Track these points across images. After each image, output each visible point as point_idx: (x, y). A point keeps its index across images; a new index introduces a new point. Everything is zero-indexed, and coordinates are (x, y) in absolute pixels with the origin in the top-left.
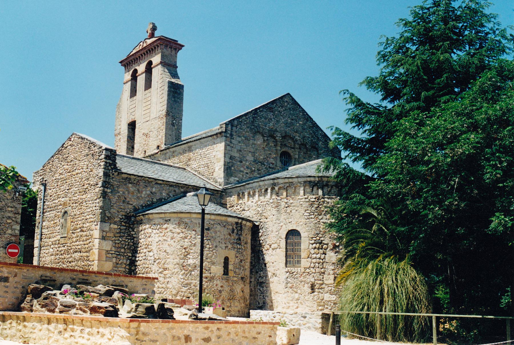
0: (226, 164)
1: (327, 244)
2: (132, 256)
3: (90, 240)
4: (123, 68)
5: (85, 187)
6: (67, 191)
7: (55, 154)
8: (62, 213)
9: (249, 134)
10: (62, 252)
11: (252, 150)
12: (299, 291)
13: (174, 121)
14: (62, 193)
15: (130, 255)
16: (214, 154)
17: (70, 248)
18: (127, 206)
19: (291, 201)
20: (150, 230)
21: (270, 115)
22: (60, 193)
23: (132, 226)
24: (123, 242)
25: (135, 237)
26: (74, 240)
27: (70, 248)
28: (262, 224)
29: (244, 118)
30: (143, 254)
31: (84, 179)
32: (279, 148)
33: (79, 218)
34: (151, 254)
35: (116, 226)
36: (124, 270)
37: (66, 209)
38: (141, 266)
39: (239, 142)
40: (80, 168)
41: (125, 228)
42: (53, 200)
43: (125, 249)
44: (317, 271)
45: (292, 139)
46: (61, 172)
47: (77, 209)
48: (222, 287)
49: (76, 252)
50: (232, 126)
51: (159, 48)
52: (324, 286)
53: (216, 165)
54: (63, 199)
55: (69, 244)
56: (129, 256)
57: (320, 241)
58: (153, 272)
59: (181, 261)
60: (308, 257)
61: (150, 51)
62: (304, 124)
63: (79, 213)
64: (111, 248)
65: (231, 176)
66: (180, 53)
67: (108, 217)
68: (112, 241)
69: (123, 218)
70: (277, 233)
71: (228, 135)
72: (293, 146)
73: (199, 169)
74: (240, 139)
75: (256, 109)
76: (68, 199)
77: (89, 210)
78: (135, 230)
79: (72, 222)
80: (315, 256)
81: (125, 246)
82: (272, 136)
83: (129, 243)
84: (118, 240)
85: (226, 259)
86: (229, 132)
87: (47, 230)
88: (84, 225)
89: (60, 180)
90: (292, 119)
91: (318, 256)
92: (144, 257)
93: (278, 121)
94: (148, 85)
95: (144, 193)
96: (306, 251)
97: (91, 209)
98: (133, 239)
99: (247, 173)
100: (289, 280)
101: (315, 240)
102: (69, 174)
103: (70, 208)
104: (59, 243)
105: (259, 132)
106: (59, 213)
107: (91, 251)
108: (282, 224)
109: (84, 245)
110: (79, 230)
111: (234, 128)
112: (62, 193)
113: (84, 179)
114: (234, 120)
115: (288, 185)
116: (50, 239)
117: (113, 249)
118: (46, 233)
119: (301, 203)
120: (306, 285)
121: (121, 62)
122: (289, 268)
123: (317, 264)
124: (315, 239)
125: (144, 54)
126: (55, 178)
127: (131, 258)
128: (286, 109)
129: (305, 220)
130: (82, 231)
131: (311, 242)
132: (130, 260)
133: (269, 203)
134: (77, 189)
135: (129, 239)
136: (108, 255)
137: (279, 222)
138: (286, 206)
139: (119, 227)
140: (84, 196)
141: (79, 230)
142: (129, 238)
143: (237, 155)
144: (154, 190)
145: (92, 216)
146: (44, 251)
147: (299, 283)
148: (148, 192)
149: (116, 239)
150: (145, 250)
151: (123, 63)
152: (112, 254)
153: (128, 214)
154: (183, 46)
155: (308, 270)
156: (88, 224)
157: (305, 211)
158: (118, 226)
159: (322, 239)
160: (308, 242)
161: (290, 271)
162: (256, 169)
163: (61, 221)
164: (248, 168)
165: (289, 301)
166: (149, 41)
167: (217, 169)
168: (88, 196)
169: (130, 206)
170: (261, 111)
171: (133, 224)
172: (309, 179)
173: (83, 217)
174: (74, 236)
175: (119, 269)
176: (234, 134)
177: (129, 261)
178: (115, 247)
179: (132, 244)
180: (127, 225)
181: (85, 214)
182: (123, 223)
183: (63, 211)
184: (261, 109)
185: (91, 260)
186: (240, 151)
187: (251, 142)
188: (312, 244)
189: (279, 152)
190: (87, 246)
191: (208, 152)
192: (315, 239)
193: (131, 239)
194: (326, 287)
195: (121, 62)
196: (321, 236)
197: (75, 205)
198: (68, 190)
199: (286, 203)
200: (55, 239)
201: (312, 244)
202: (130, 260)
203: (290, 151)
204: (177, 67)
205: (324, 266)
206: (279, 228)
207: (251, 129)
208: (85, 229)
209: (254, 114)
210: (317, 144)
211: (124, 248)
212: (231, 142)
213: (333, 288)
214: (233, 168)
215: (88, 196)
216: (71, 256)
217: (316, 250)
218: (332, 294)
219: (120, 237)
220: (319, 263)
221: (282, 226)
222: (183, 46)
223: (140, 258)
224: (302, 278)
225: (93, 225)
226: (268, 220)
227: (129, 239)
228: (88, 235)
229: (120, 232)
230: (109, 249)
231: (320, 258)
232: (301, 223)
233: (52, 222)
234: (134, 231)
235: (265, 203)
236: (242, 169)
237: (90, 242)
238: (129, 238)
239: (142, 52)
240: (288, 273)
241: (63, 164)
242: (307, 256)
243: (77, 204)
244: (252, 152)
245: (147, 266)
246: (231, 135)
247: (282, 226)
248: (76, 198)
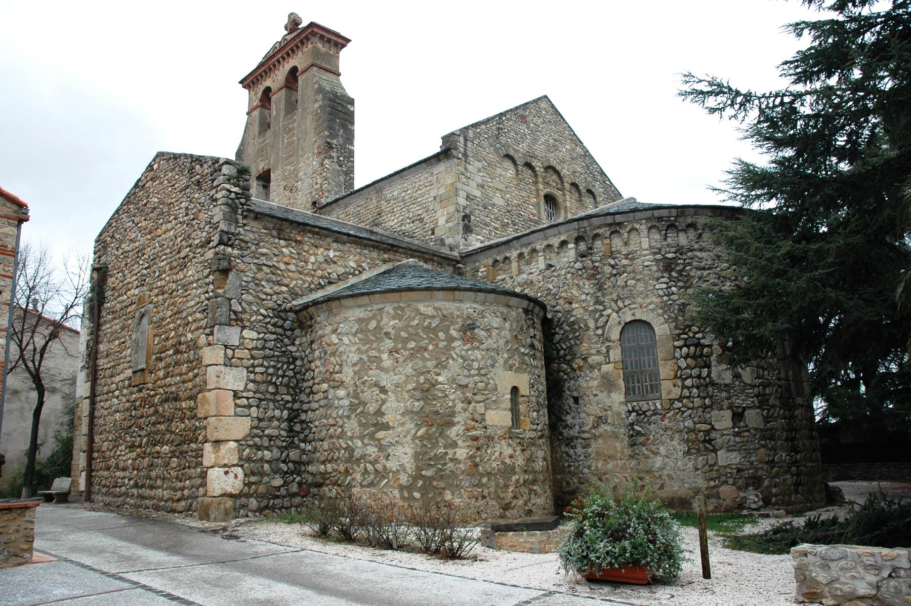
0: (462, 208)
1: (710, 346)
2: (294, 401)
3: (196, 371)
4: (247, 91)
5: (182, 254)
6: (145, 272)
7: (122, 205)
8: (136, 320)
9: (493, 157)
10: (137, 403)
11: (502, 187)
12: (662, 450)
13: (341, 159)
14: (134, 278)
15: (289, 398)
16: (433, 194)
17: (152, 393)
18: (276, 288)
19: (625, 262)
20: (334, 339)
21: (523, 128)
22: (131, 280)
23: (288, 333)
24: (271, 371)
25: (295, 359)
26: (161, 374)
27: (152, 393)
28: (560, 315)
29: (483, 127)
30: (321, 395)
31: (179, 239)
32: (541, 186)
33: (171, 325)
34: (341, 393)
35: (254, 335)
36: (275, 432)
37: (143, 310)
38: (317, 423)
39: (479, 171)
40: (172, 217)
41: (274, 337)
42: (119, 296)
43: (277, 386)
44: (696, 405)
45: (557, 173)
46: (133, 235)
47: (166, 304)
48: (511, 457)
49: (167, 400)
50: (466, 140)
51: (309, 43)
52: (713, 435)
53: (439, 213)
54: (137, 291)
55: (150, 386)
56: (287, 402)
57: (695, 341)
58: (349, 434)
59: (416, 404)
60: (676, 377)
61: (293, 51)
62: (573, 150)
63: (169, 313)
64: (247, 384)
65: (471, 232)
66: (343, 53)
67: (235, 313)
68: (247, 368)
69: (269, 316)
70: (599, 332)
71: (460, 156)
72: (559, 186)
73: (403, 228)
74: (477, 164)
75: (501, 115)
76: (145, 288)
77: (192, 303)
78: (297, 342)
79: (155, 336)
80: (688, 371)
81: (278, 378)
82: (528, 165)
83: (284, 372)
84: (262, 365)
85: (515, 390)
86: (462, 150)
87: (106, 361)
88: (183, 339)
89: (131, 254)
90: (556, 140)
91: (695, 372)
92: (322, 403)
93: (535, 141)
94: (291, 107)
95: (312, 259)
96: (670, 363)
97: (197, 299)
98: (293, 363)
99: (496, 229)
100: (637, 428)
101: (685, 340)
102: (149, 237)
103: (152, 306)
104: (130, 386)
105: (508, 156)
106: (130, 322)
107: (200, 396)
108: (609, 311)
109: (184, 382)
110: (171, 352)
111: (469, 144)
112: (134, 278)
113: (179, 239)
114: (467, 128)
115: (613, 229)
116: (113, 379)
117: (251, 386)
118: (106, 366)
119: (646, 263)
120: (677, 436)
121: (241, 82)
122: (635, 404)
123: (695, 390)
124: (686, 336)
125: (284, 59)
126: (121, 251)
127: (289, 405)
128: (544, 122)
129: (659, 300)
130: (177, 352)
131: (676, 343)
132: (289, 409)
133: (573, 270)
134: (165, 262)
135: (284, 363)
136: (238, 401)
137: (601, 308)
138: (614, 272)
139: (261, 336)
140: (181, 275)
141: (171, 352)
142: (285, 360)
143: (477, 193)
144: (331, 254)
145: (198, 315)
146: (102, 404)
147: (662, 432)
148: (321, 259)
149: (256, 362)
150: (325, 386)
151: (246, 83)
152: (248, 398)
153: (280, 305)
154: (348, 41)
155: (678, 405)
156: (189, 336)
157: (658, 279)
158: (259, 333)
159: (700, 335)
160: (671, 344)
161: (637, 408)
162: (510, 222)
163: (134, 337)
164: (496, 219)
165: (642, 475)
166: (289, 37)
167: (442, 221)
168: (190, 273)
169: (284, 289)
170: (507, 119)
171: (292, 330)
172: (657, 213)
173: (178, 322)
174: (161, 365)
175: (267, 432)
176: (469, 153)
177: (286, 412)
178: (252, 381)
179: (291, 373)
180: (280, 330)
181: (184, 314)
182: (269, 326)
183: (137, 315)
184: (508, 116)
185: (199, 415)
186: (483, 187)
187: (499, 171)
188: (681, 348)
189: (542, 194)
190: (190, 385)
191: (419, 192)
192: (686, 336)
193: (289, 363)
194: (718, 436)
195: (241, 82)
196: (697, 329)
197: (161, 297)
198: (146, 269)
199: (613, 267)
200: (122, 376)
201: (681, 348)
202: (289, 409)
203: (558, 194)
204: (339, 75)
205: (710, 394)
206: (603, 319)
207: (496, 150)
208: (183, 348)
209: (499, 124)
210: (594, 186)
211: (275, 383)
212: (466, 169)
213: (732, 438)
214: (472, 217)
215: (190, 273)
216: (157, 411)
217: (689, 360)
218: (731, 451)
219: (264, 358)
220: (698, 388)
221: (609, 316)
222: (348, 41)
223: (314, 405)
224: (666, 421)
225: (203, 336)
226: (574, 306)
227: (284, 363)
228: (192, 357)
229: (264, 348)
230: (241, 388)
231: (699, 377)
232: (652, 306)
233: (117, 342)
234: (293, 344)
235: (563, 272)
236: (487, 220)
237: (196, 376)
238: (285, 360)
239: (279, 56)
240: (634, 414)
241: (136, 220)
242: (672, 374)
243: (166, 295)
244: (501, 190)
245: (331, 421)
246: (465, 155)
247: (609, 316)
248: (163, 283)
